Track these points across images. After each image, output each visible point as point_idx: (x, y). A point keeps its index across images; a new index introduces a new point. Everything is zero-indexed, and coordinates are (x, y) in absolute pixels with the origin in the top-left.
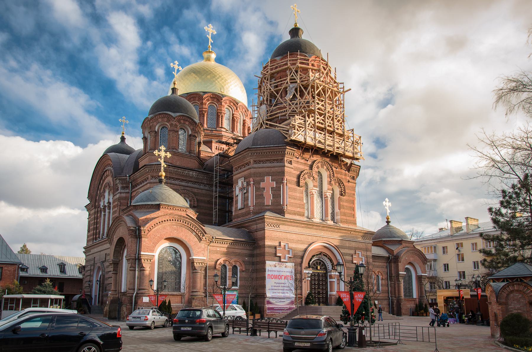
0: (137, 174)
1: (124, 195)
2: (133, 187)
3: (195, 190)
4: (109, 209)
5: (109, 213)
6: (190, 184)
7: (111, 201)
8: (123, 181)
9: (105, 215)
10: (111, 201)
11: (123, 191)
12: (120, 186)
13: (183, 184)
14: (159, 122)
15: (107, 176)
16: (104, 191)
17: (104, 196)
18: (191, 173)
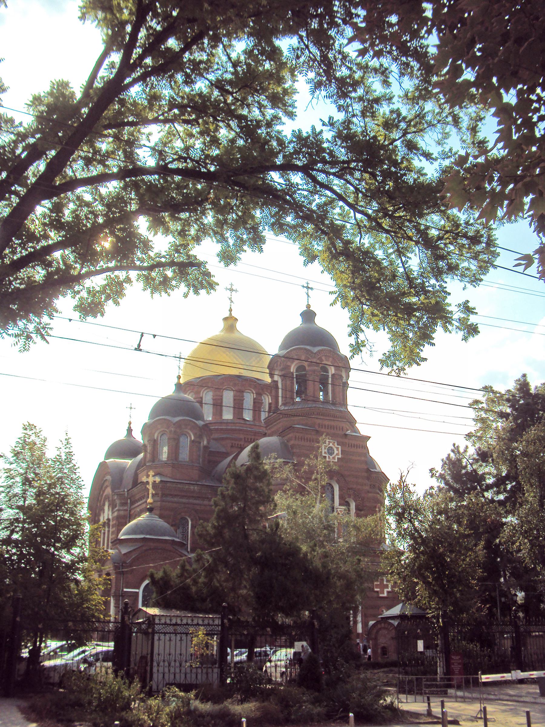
0: (135, 490)
1: (122, 513)
2: (132, 503)
3: (198, 508)
4: (109, 527)
5: (109, 531)
6: (191, 501)
7: (110, 517)
8: (120, 496)
9: (104, 533)
10: (110, 517)
11: (121, 508)
12: (118, 502)
13: (184, 500)
14: (158, 429)
15: (106, 487)
16: (104, 505)
17: (104, 510)
18: (192, 487)
